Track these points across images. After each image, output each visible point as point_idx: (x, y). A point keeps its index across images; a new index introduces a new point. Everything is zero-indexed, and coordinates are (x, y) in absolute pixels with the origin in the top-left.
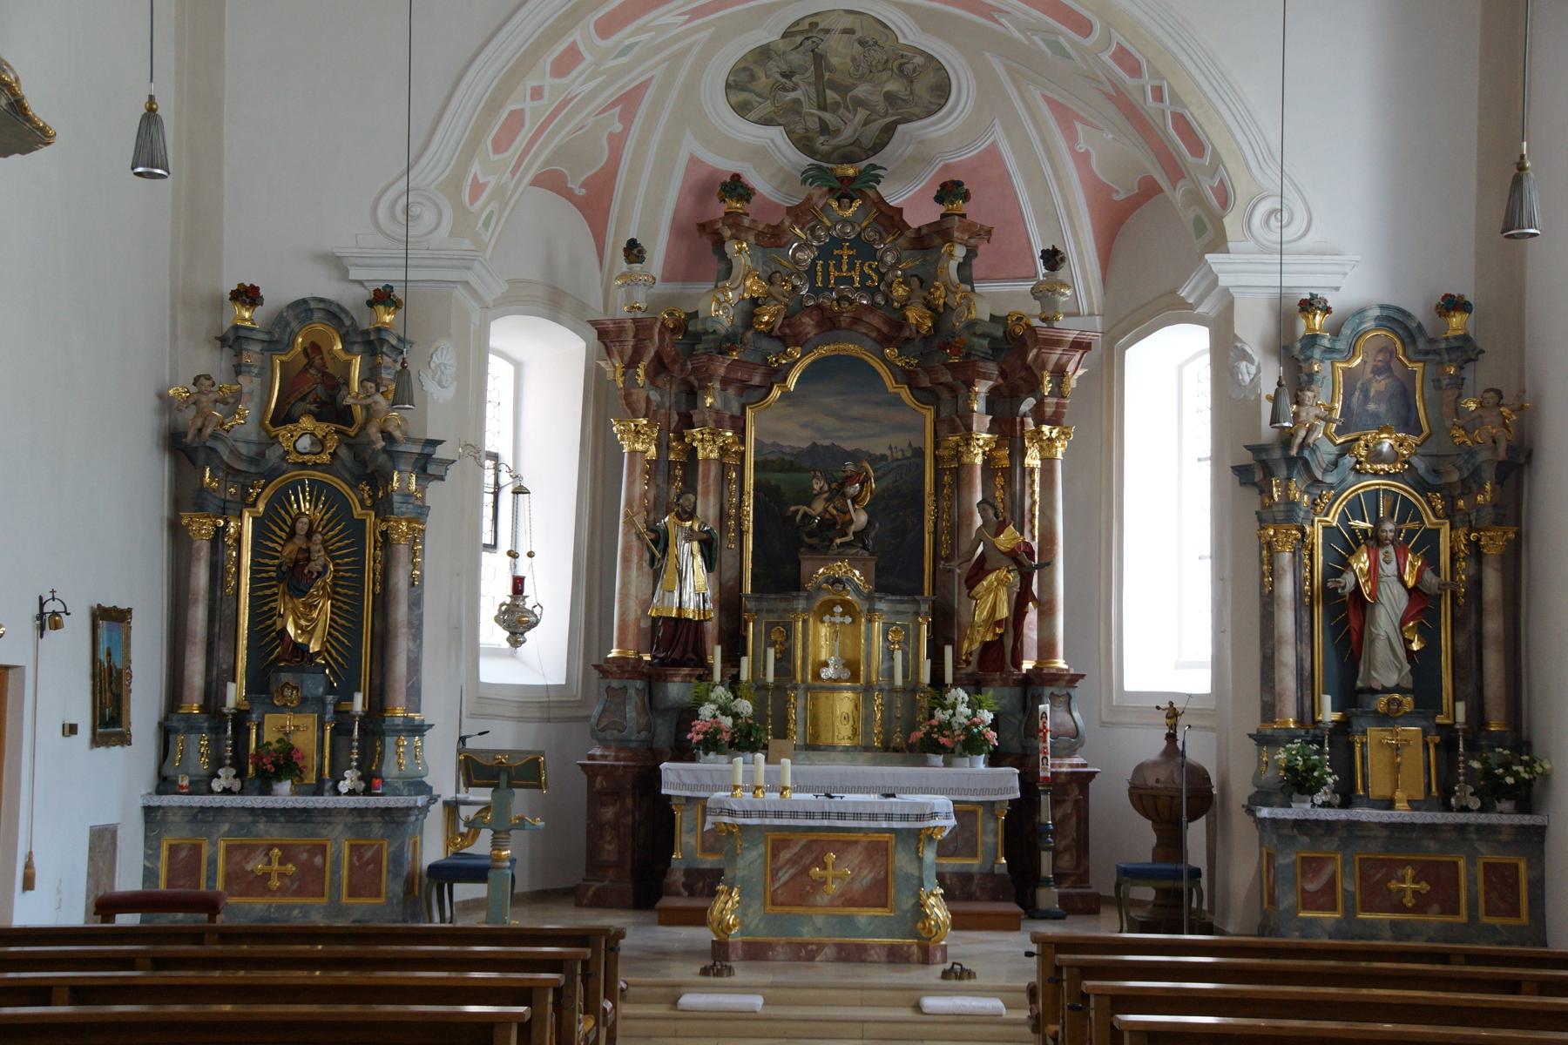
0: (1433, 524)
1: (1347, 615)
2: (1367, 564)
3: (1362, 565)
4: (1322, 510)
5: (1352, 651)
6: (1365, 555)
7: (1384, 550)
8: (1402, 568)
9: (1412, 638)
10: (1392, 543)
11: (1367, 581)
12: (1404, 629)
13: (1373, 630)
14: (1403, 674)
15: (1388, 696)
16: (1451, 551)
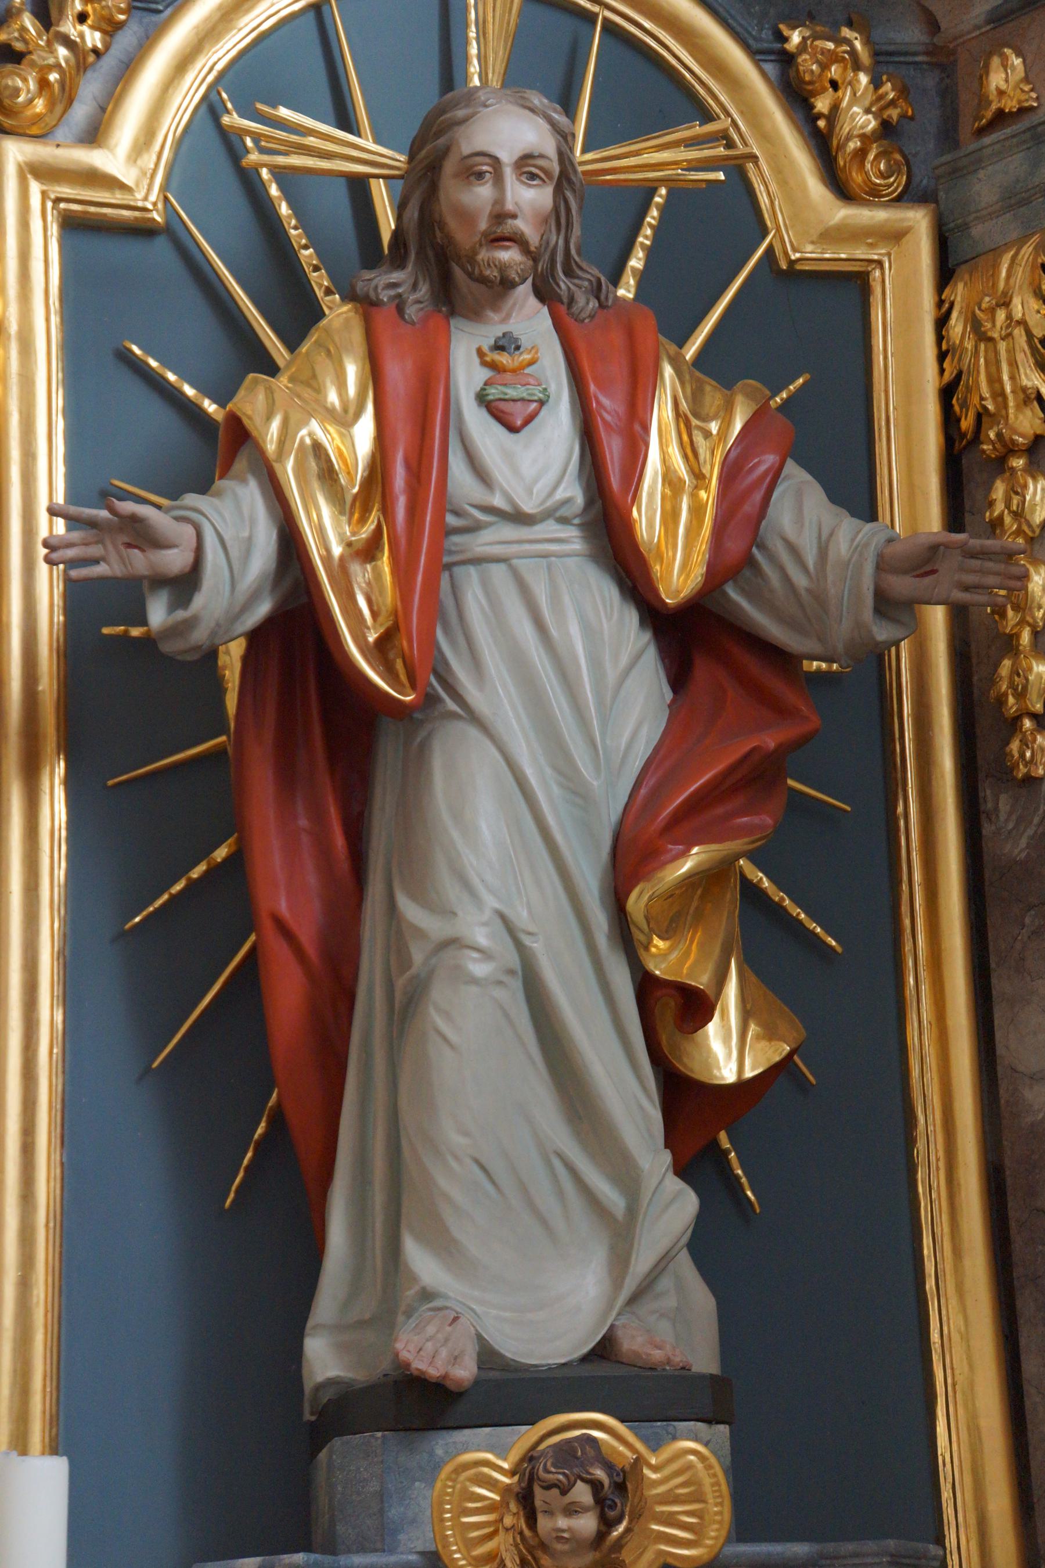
0: (831, 235)
1: (236, 859)
2: (364, 431)
3: (329, 438)
4: (67, 95)
5: (278, 1119)
6: (352, 371)
7: (486, 334)
8: (613, 448)
9: (702, 981)
10: (544, 293)
11: (368, 552)
12: (637, 902)
13: (410, 910)
14: (642, 1263)
15: (524, 1437)
16: (949, 420)
